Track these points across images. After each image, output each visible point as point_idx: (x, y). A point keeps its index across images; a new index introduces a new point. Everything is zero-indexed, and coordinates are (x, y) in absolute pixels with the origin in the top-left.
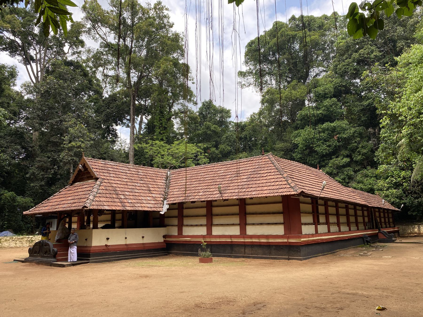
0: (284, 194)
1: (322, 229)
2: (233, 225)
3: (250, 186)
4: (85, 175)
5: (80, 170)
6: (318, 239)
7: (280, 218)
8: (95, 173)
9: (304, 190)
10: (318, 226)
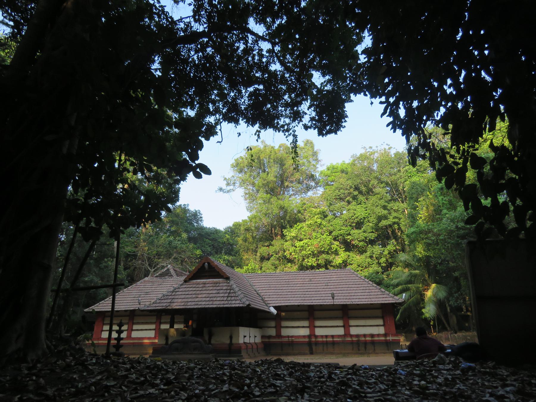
7: (380, 322)
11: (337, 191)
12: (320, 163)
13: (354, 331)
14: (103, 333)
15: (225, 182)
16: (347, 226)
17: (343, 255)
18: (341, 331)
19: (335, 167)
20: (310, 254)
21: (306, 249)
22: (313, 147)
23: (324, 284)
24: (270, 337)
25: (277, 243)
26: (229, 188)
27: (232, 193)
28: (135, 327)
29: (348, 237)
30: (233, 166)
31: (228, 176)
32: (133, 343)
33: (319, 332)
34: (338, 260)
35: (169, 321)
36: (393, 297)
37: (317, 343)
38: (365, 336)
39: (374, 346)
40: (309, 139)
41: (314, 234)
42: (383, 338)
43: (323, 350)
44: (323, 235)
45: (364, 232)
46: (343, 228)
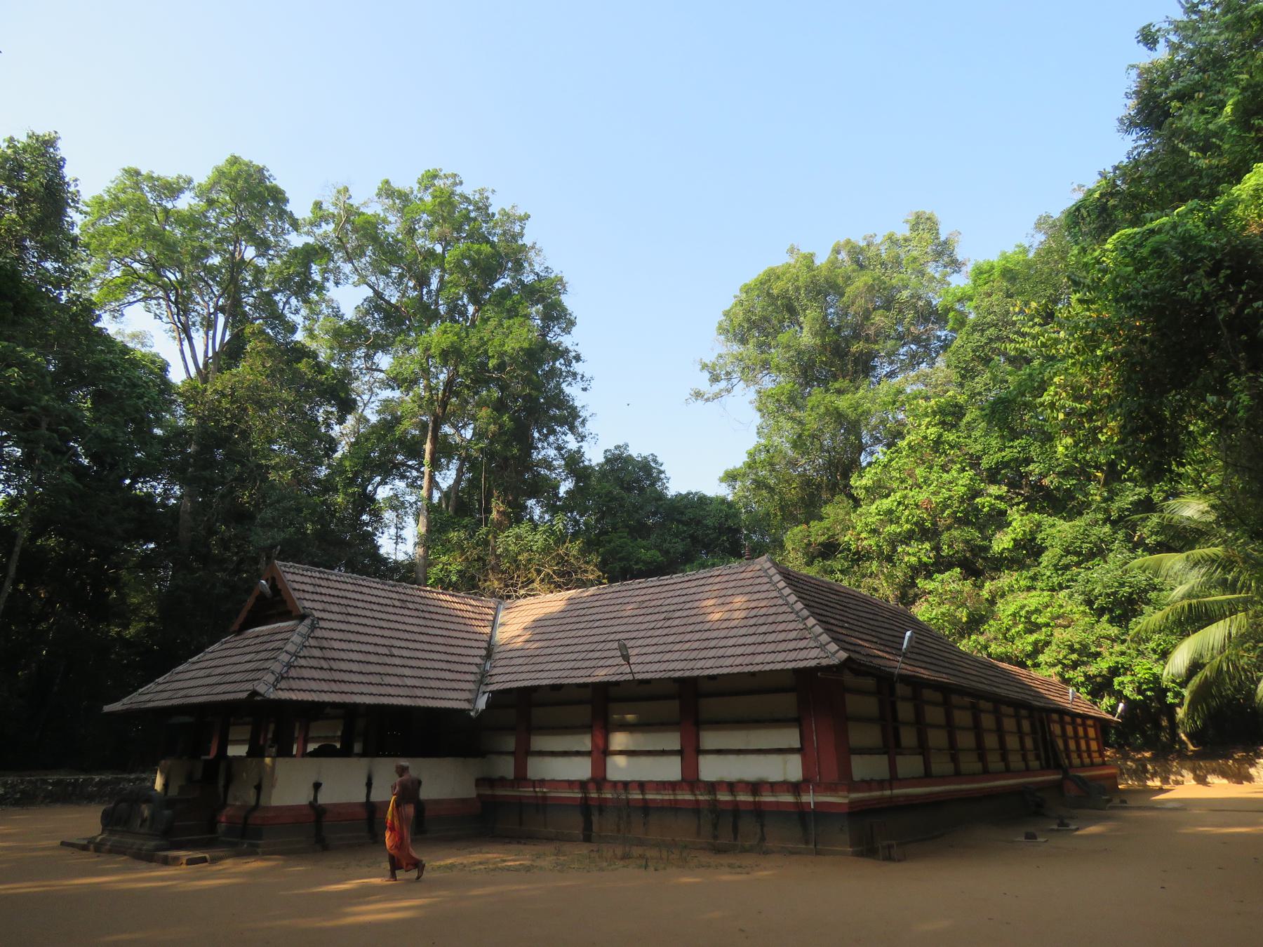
0: (801, 665)
1: (910, 765)
2: (663, 753)
3: (713, 643)
4: (276, 606)
5: (262, 596)
6: (898, 796)
7: (791, 737)
8: (298, 602)
9: (854, 656)
10: (900, 760)
12: (964, 269)
13: (711, 769)
15: (706, 375)
17: (1019, 522)
18: (670, 769)
19: (986, 267)
20: (911, 532)
21: (899, 518)
23: (663, 616)
24: (502, 781)
25: (833, 511)
26: (717, 387)
27: (727, 398)
29: (1031, 468)
30: (722, 330)
31: (710, 358)
33: (619, 768)
34: (1002, 542)
35: (339, 733)
36: (822, 647)
37: (602, 806)
38: (732, 786)
39: (762, 826)
40: (921, 210)
41: (920, 472)
42: (789, 798)
43: (619, 831)
44: (947, 472)
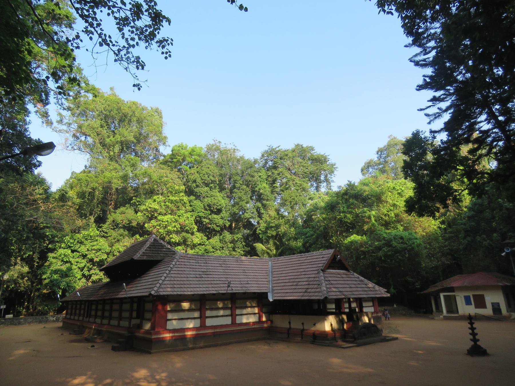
11: (206, 176)
14: (168, 322)
16: (206, 210)
20: (174, 231)
22: (161, 117)
28: (208, 313)
32: (214, 333)
34: (196, 241)
45: (222, 218)
46: (203, 211)
